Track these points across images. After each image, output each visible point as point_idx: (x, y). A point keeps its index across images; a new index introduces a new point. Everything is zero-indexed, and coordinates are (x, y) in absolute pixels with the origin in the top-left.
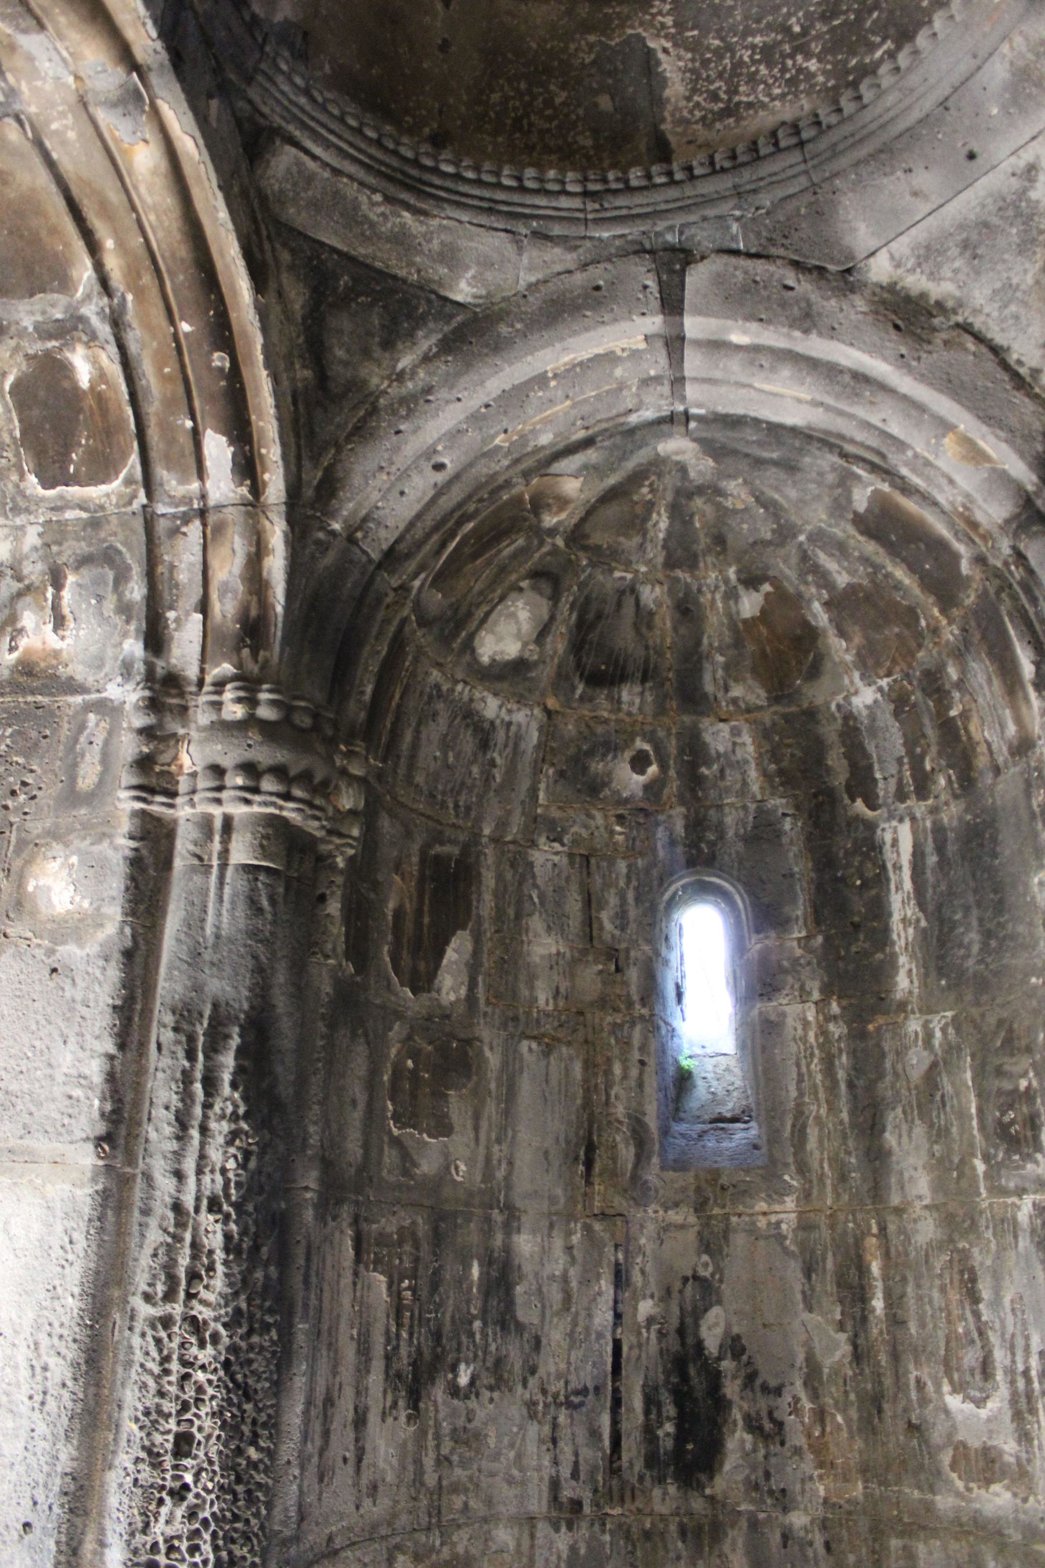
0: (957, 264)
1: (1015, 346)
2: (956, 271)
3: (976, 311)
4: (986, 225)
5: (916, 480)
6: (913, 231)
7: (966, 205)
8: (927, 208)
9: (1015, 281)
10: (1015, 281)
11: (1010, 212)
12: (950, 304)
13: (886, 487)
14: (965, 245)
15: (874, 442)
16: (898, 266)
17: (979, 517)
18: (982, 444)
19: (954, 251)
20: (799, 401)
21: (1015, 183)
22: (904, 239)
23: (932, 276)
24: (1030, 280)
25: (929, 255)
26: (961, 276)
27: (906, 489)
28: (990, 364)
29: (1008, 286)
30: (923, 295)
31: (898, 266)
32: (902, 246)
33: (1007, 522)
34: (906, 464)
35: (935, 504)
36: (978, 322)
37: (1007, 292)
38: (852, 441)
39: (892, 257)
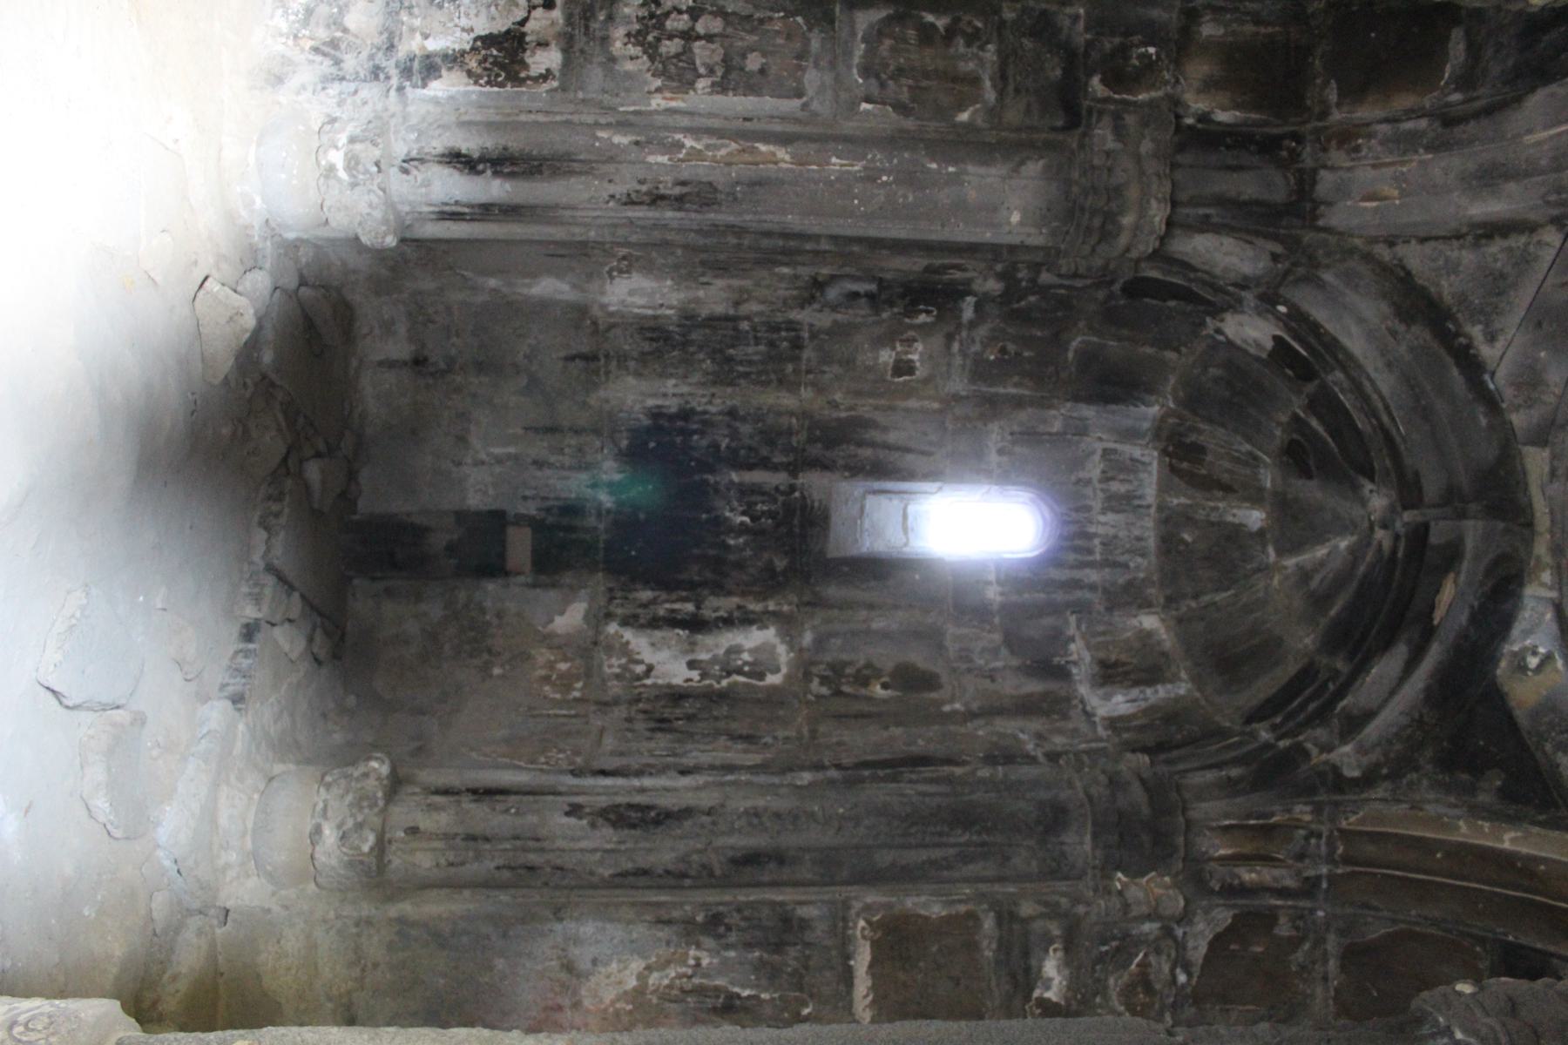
0: (1499, 264)
1: (1419, 247)
2: (1496, 260)
3: (1462, 247)
4: (1499, 294)
5: (1408, 125)
6: (1546, 265)
7: (1523, 297)
8: (1549, 282)
9: (1453, 277)
10: (1453, 277)
11: (1488, 309)
12: (1483, 241)
13: (1427, 102)
14: (1503, 276)
15: (1459, 131)
16: (1539, 242)
17: (1337, 157)
18: (1374, 204)
19: (1508, 269)
20: (1530, 131)
21: (1497, 325)
22: (1550, 258)
23: (1510, 250)
24: (1444, 283)
25: (1524, 261)
26: (1490, 259)
27: (1412, 114)
28: (1422, 234)
29: (1456, 272)
30: (1505, 236)
31: (1539, 242)
32: (1548, 255)
33: (1314, 183)
34: (1423, 133)
35: (1387, 120)
36: (1455, 243)
37: (1452, 268)
38: (1476, 115)
39: (1548, 244)
